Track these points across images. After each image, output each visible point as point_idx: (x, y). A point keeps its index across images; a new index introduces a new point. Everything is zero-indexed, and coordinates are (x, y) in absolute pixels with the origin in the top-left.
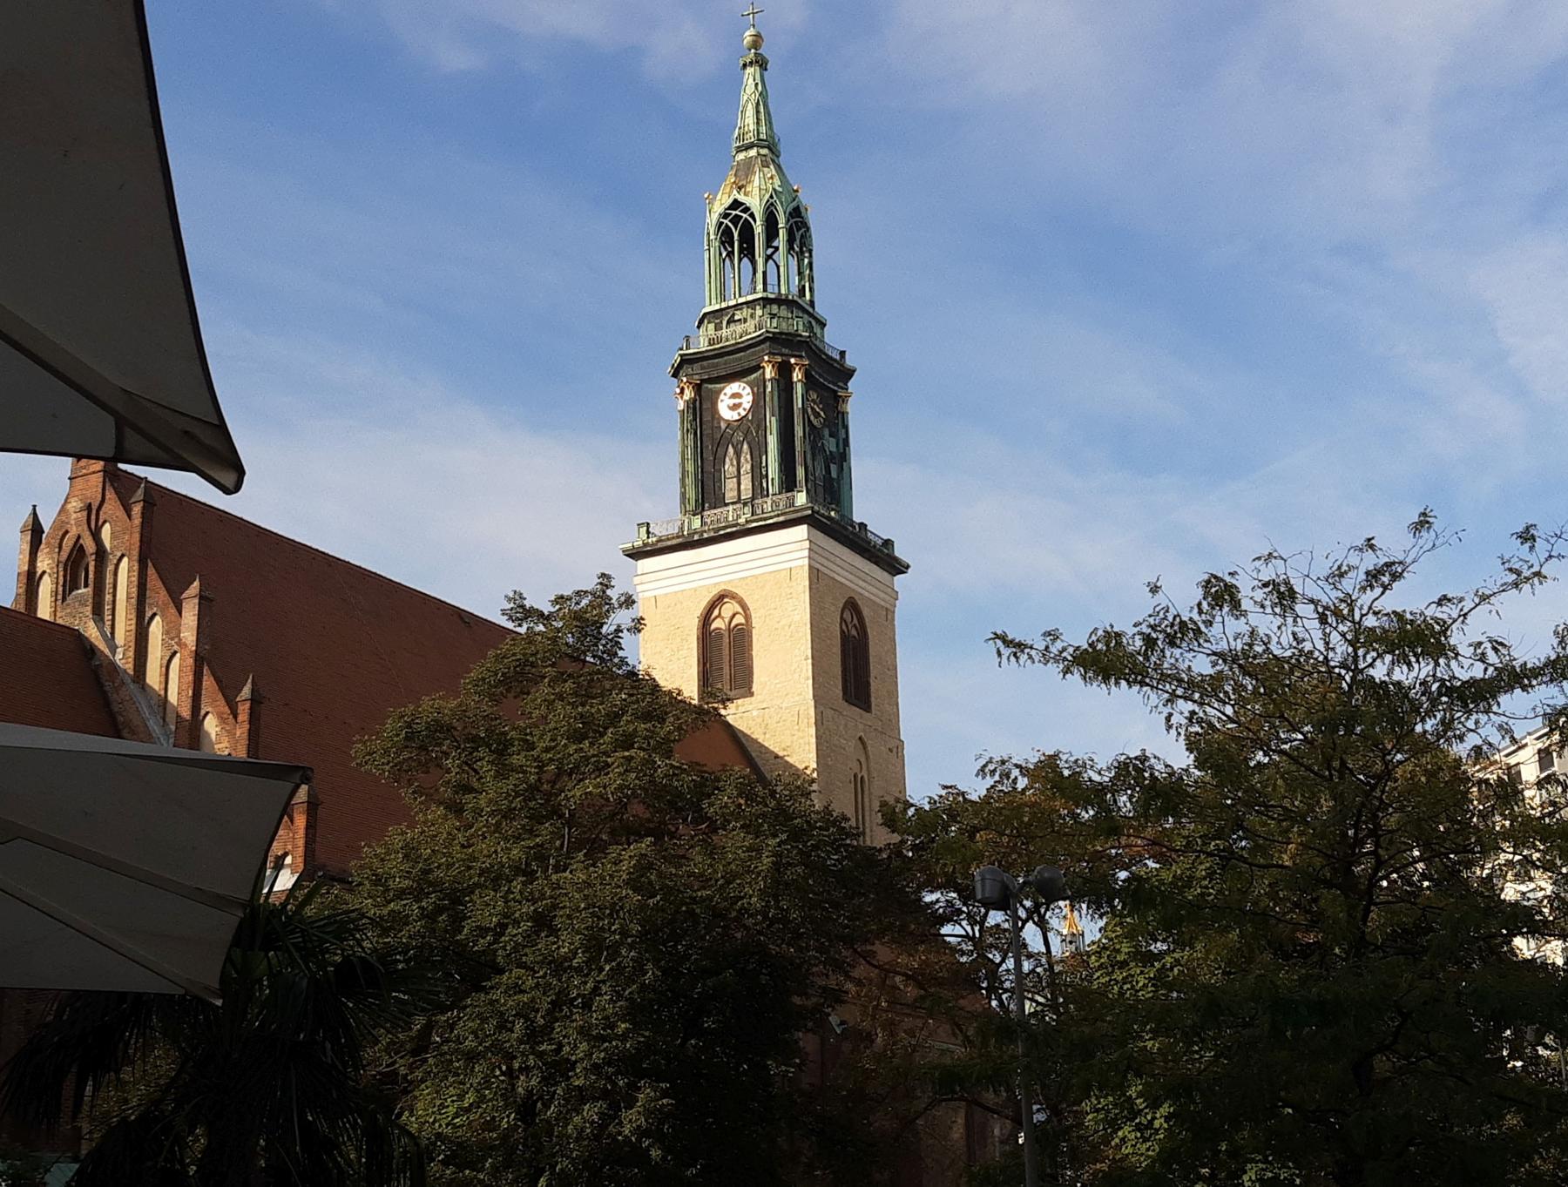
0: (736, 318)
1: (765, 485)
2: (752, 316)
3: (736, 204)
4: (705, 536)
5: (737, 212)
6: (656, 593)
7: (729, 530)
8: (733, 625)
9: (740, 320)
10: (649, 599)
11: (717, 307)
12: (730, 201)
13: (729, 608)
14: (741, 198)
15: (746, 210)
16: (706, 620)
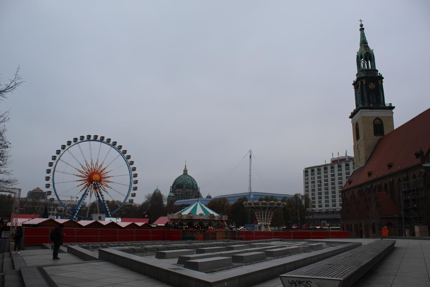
0: (371, 72)
1: (379, 101)
2: (374, 72)
3: (367, 53)
4: (376, 108)
5: (368, 54)
6: (365, 115)
7: (380, 108)
8: (379, 123)
9: (371, 72)
10: (363, 116)
11: (367, 69)
12: (367, 52)
13: (377, 121)
14: (368, 52)
15: (370, 54)
16: (374, 121)
